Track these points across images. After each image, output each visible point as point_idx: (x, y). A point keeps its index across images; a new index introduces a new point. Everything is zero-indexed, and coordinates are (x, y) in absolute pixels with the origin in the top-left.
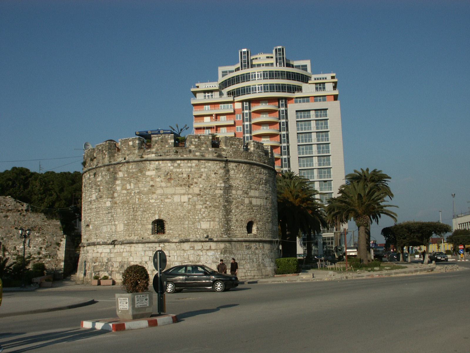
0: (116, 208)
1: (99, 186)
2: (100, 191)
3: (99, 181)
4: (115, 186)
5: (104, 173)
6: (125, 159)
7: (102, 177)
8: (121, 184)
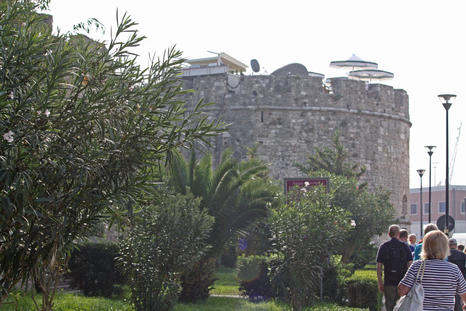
0: (378, 175)
1: (351, 139)
2: (354, 146)
3: (353, 133)
4: (376, 145)
5: (361, 124)
6: (385, 112)
7: (359, 127)
8: (383, 143)
